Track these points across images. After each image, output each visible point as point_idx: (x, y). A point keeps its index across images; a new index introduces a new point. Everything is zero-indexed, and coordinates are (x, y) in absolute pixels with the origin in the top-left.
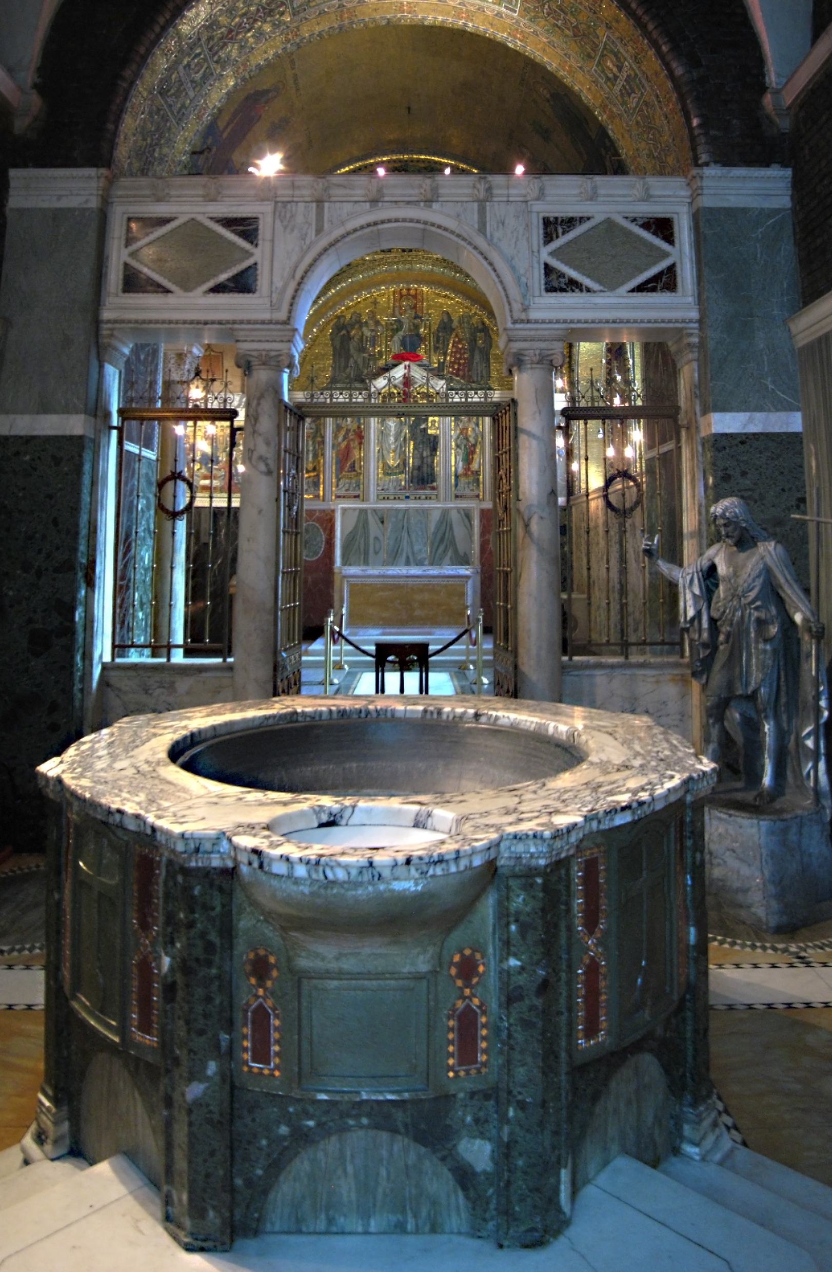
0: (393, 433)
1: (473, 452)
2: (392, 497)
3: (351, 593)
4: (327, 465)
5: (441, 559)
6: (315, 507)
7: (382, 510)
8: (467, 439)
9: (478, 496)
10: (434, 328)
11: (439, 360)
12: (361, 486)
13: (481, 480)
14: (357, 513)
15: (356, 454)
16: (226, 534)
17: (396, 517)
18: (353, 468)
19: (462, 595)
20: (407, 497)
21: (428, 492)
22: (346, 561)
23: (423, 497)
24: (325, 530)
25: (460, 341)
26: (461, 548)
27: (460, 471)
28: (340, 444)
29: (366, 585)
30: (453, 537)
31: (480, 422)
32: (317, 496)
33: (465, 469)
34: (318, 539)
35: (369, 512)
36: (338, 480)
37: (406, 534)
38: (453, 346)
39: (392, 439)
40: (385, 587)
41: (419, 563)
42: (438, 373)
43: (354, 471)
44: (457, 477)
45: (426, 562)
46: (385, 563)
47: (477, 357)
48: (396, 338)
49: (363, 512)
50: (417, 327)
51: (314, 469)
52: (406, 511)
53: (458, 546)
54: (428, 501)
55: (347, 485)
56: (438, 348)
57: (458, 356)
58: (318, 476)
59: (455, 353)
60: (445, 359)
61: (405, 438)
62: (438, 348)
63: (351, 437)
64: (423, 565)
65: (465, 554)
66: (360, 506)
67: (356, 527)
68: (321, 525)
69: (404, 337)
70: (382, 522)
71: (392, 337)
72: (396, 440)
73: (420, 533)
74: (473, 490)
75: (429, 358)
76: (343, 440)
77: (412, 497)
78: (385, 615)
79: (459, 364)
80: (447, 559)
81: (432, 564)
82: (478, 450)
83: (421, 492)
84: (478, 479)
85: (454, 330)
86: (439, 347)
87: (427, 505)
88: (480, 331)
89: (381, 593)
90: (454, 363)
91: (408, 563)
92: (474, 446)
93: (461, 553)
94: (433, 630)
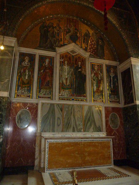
1: (100, 83)
5: (89, 129)
6: (27, 102)
7: (61, 104)
8: (97, 77)
9: (103, 101)
10: (83, 34)
13: (104, 94)
15: (48, 79)
17: (68, 108)
18: (48, 84)
20: (73, 100)
21: (82, 98)
24: (32, 113)
25: (93, 41)
26: (97, 125)
27: (95, 90)
30: (94, 118)
33: (97, 90)
35: (55, 105)
37: (73, 116)
38: (90, 42)
41: (79, 131)
43: (48, 86)
44: (94, 92)
45: (82, 130)
46: (62, 131)
48: (68, 35)
50: (77, 33)
52: (73, 105)
55: (45, 92)
59: (91, 45)
62: (85, 42)
63: (48, 71)
64: (80, 131)
70: (62, 110)
71: (66, 34)
76: (43, 72)
78: (69, 161)
79: (93, 49)
80: (91, 129)
81: (84, 131)
83: (79, 98)
84: (103, 94)
85: (90, 37)
86: (86, 41)
87: (82, 103)
90: (91, 48)
91: (74, 131)
92: (100, 80)
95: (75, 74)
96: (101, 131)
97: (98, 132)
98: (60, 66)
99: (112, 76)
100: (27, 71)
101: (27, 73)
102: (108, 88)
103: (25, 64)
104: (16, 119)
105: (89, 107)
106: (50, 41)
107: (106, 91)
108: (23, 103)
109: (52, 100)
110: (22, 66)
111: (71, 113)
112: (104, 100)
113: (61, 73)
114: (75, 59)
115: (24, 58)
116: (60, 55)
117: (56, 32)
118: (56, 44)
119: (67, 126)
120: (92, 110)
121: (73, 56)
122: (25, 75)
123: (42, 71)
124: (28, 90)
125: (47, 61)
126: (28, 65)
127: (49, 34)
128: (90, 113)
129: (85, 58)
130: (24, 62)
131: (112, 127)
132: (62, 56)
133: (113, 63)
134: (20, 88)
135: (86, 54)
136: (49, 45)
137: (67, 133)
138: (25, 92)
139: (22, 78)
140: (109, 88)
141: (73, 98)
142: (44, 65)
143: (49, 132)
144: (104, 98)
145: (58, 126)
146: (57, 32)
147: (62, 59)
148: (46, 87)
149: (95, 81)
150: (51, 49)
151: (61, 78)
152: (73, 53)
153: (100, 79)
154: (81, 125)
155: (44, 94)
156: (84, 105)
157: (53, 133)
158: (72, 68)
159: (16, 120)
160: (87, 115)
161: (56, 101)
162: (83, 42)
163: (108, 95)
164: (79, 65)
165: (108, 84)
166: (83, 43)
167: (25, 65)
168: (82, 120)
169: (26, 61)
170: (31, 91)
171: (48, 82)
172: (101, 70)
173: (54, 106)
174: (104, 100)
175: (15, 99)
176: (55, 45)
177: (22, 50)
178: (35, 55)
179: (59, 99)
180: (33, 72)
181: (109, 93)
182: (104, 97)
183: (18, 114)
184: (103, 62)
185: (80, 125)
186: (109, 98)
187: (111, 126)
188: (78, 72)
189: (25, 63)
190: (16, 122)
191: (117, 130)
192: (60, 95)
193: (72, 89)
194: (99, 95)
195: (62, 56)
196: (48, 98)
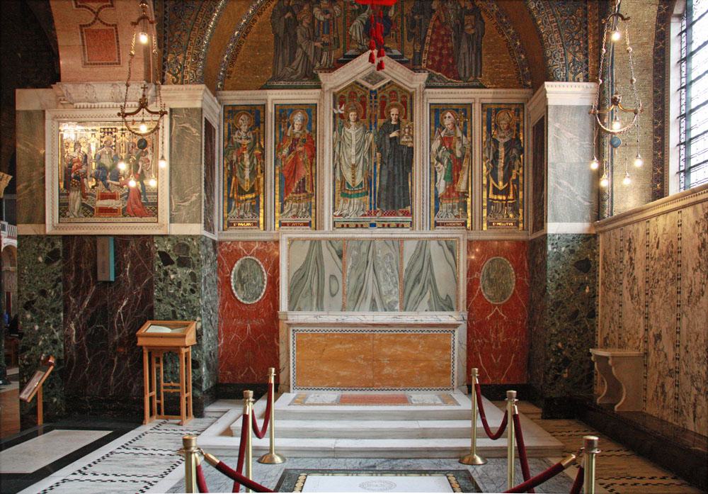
0: (354, 142)
1: (460, 168)
2: (353, 224)
3: (299, 345)
4: (268, 185)
8: (452, 151)
9: (465, 224)
11: (414, 50)
12: (313, 211)
13: (469, 203)
14: (308, 242)
15: (304, 172)
16: (131, 270)
17: (359, 249)
18: (301, 188)
19: (447, 348)
20: (373, 225)
21: (400, 218)
22: (293, 306)
23: (394, 224)
27: (441, 191)
28: (285, 157)
29: (319, 336)
30: (432, 274)
31: (469, 131)
32: (257, 224)
33: (447, 190)
34: (259, 278)
35: (323, 243)
36: (283, 203)
38: (433, 32)
39: (353, 151)
40: (344, 338)
41: (389, 308)
42: (414, 66)
43: (305, 191)
44: (437, 199)
45: (397, 307)
46: (344, 308)
47: (465, 46)
49: (315, 243)
51: (252, 190)
52: (372, 241)
53: (439, 287)
54: (399, 230)
55: (295, 210)
56: (414, 34)
57: (440, 45)
58: (257, 198)
59: (437, 40)
60: (422, 49)
61: (370, 149)
64: (392, 309)
65: (447, 295)
66: (313, 236)
67: (307, 259)
68: (262, 262)
69: (369, 20)
70: (340, 256)
71: (353, 21)
72: (358, 152)
73: (389, 270)
74: (458, 216)
75: (401, 48)
76: (289, 153)
77: (379, 225)
79: (441, 55)
80: (424, 303)
82: (465, 165)
83: (392, 218)
84: (466, 202)
85: (433, 11)
87: (398, 233)
88: (468, 13)
89: (338, 346)
90: (434, 53)
91: (373, 307)
92: (460, 160)
93: (442, 294)
94: (408, 393)
95: (379, 149)
96: (452, 309)
97: (444, 310)
98: (334, 130)
99: (502, 141)
100: (246, 157)
101: (248, 163)
102: (485, 182)
103: (241, 139)
104: (232, 280)
105: (418, 245)
106: (305, 53)
107: (477, 188)
108: (244, 242)
109: (316, 229)
110: (233, 144)
111: (368, 262)
112: (469, 221)
113: (337, 151)
114: (378, 100)
115: (237, 122)
116: (334, 95)
117: (319, 21)
118: (320, 62)
119: (356, 298)
120: (427, 252)
121: (375, 91)
122: (243, 170)
123: (285, 152)
124: (252, 207)
125: (298, 119)
126: (248, 139)
127: (298, 32)
128: (422, 255)
129: (411, 91)
130: (237, 133)
131: (487, 295)
132: (339, 99)
133: (513, 95)
134: (233, 205)
135: (415, 77)
136: (300, 69)
137: (355, 313)
138: (246, 213)
139: (236, 177)
140: (488, 182)
141: (373, 221)
142: (289, 134)
143: (311, 310)
144: (469, 214)
145: (333, 295)
146: (322, 18)
147: (338, 106)
148: (298, 195)
149: (442, 163)
150: (307, 79)
151: (338, 166)
152: (374, 83)
153: (458, 154)
154: (393, 292)
155: (294, 216)
156: (402, 240)
157: (320, 313)
158: (370, 132)
159: (233, 284)
160: (412, 265)
161: (327, 231)
162: (408, 31)
163: (485, 204)
164: (393, 117)
165: (488, 170)
166: (406, 37)
167: (240, 141)
168: (398, 280)
169: (242, 127)
170: (262, 211)
171: (304, 179)
172: (465, 123)
173: (320, 246)
174: (469, 221)
175: (225, 232)
176: (318, 65)
177: (228, 98)
178: (264, 106)
179: (334, 226)
180: (263, 156)
181: (488, 196)
182: (469, 211)
183: (234, 269)
184: (472, 96)
185: (390, 292)
186: (485, 215)
187: (484, 295)
188: (388, 141)
189: (239, 134)
190: (233, 288)
191: (505, 308)
192: (336, 213)
193: (371, 196)
194: (453, 207)
195: (339, 99)
196: (305, 224)
